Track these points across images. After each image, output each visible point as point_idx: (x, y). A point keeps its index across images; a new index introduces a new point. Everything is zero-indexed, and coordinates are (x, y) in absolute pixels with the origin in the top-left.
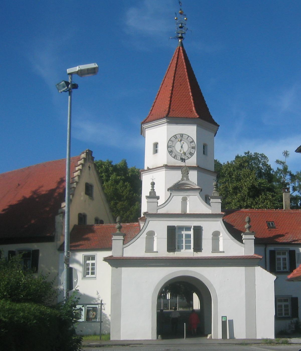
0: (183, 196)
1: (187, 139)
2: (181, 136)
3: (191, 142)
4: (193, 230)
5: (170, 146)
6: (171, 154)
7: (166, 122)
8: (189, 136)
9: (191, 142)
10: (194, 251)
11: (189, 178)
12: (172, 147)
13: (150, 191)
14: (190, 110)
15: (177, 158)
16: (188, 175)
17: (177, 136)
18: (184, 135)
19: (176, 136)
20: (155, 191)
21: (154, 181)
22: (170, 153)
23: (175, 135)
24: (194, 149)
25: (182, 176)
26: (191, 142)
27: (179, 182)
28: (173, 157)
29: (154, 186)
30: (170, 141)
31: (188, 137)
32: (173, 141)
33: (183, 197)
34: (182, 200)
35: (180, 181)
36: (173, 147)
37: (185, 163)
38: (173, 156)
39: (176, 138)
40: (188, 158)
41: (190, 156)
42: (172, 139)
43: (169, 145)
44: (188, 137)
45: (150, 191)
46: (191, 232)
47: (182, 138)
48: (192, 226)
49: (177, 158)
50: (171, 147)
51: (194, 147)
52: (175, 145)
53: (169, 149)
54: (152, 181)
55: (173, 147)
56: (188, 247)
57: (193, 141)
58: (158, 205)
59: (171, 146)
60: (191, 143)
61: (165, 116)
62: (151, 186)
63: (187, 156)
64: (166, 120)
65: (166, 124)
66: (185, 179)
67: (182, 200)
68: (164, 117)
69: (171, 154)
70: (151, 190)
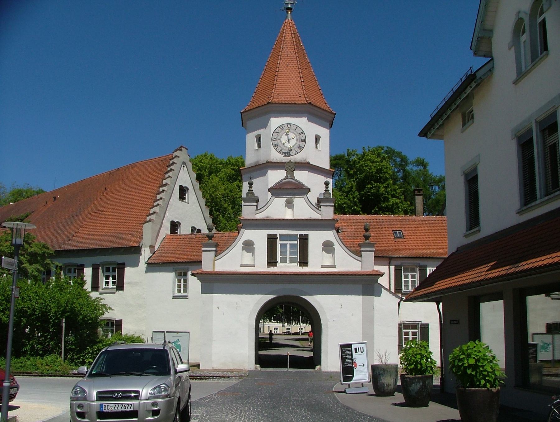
6: (276, 148)
8: (297, 127)
9: (300, 134)
10: (300, 265)
11: (295, 176)
12: (277, 140)
14: (300, 95)
23: (281, 126)
25: (286, 173)
26: (300, 134)
28: (279, 151)
33: (287, 199)
35: (283, 179)
36: (278, 139)
40: (296, 153)
42: (277, 131)
43: (274, 137)
46: (297, 242)
47: (289, 128)
48: (297, 234)
50: (276, 140)
52: (281, 137)
55: (278, 139)
56: (292, 261)
69: (276, 148)
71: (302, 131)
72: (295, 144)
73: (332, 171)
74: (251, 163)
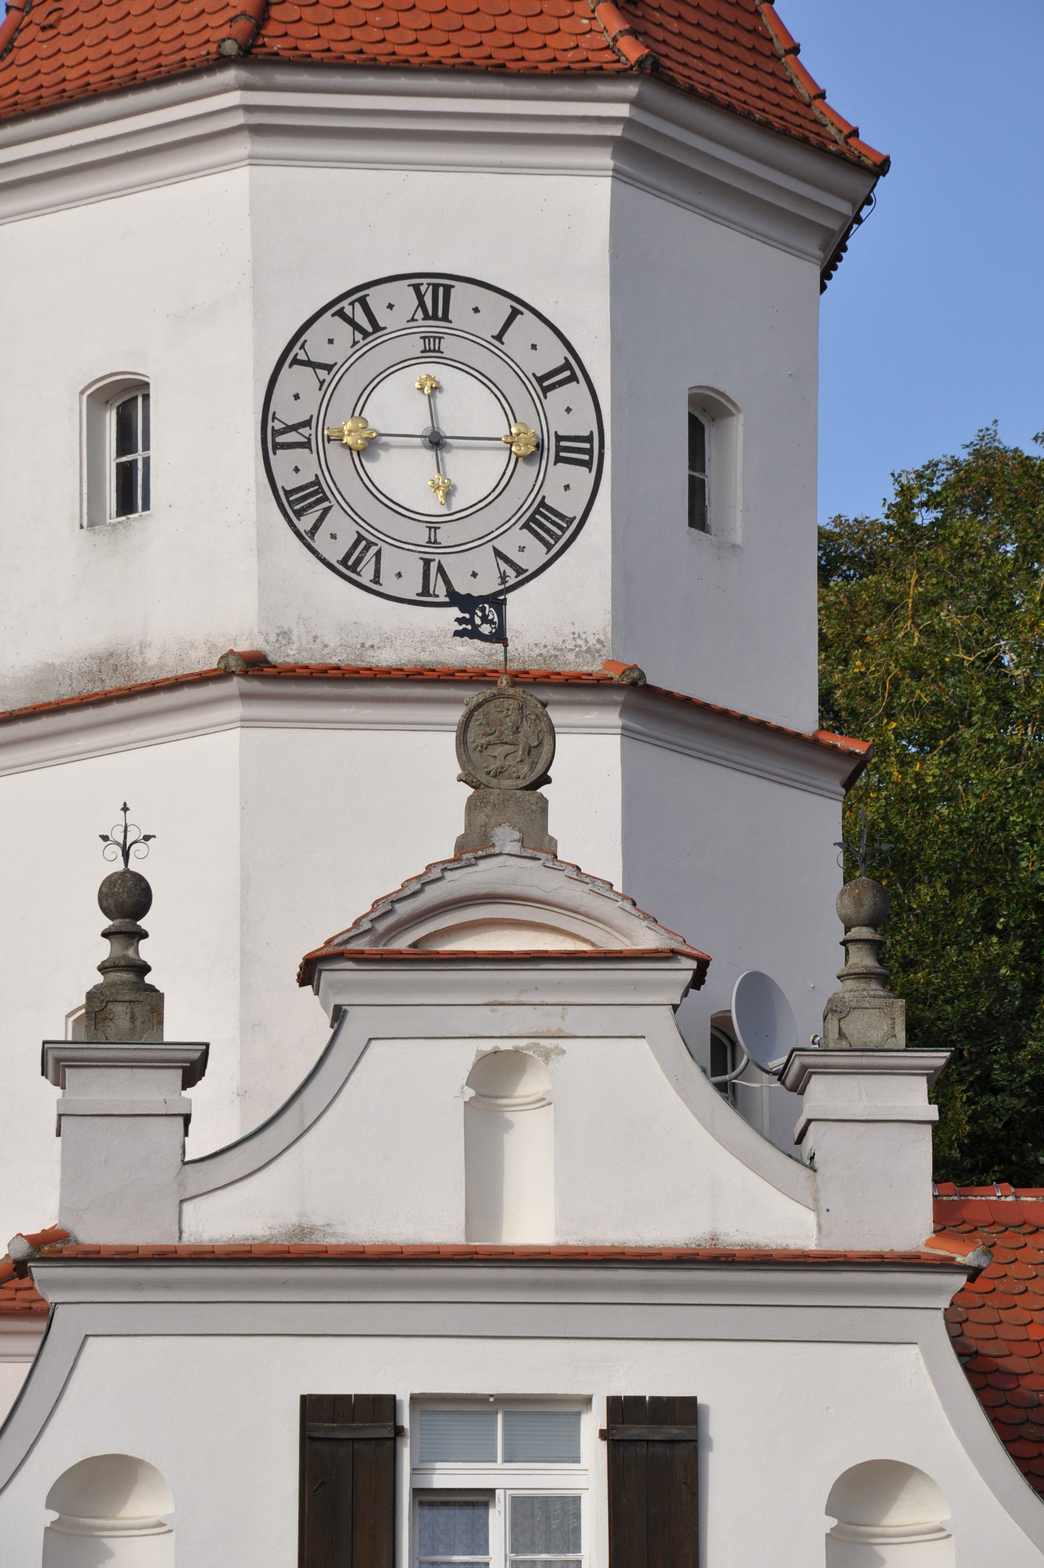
0: (488, 1046)
1: (499, 337)
2: (422, 304)
3: (540, 380)
4: (603, 1445)
5: (294, 428)
7: (239, 119)
8: (519, 307)
9: (546, 383)
11: (552, 831)
13: (99, 979)
15: (376, 580)
16: (544, 790)
17: (376, 298)
18: (459, 290)
19: (363, 302)
20: (149, 979)
21: (132, 867)
22: (299, 514)
23: (359, 294)
24: (588, 464)
26: (546, 383)
27: (436, 873)
29: (143, 923)
30: (296, 361)
31: (515, 313)
32: (328, 368)
34: (470, 1093)
37: (499, 647)
38: (335, 553)
39: (366, 334)
41: (534, 554)
44: (515, 313)
45: (99, 979)
49: (376, 580)
50: (306, 445)
51: (589, 439)
53: (282, 460)
54: (119, 866)
57: (567, 366)
58: (187, 1159)
59: (307, 423)
60: (546, 390)
61: (230, 48)
62: (106, 923)
63: (498, 553)
64: (235, 98)
65: (243, 147)
66: (506, 838)
67: (470, 1093)
68: (221, 62)
69: (305, 523)
70: (103, 969)
71: (557, 356)
72: (501, 489)
73: (851, 755)
74: (50, 667)
